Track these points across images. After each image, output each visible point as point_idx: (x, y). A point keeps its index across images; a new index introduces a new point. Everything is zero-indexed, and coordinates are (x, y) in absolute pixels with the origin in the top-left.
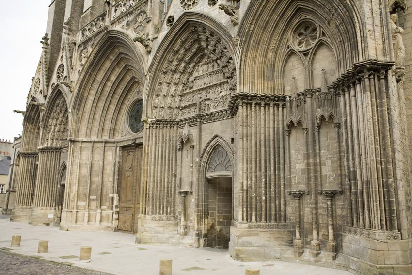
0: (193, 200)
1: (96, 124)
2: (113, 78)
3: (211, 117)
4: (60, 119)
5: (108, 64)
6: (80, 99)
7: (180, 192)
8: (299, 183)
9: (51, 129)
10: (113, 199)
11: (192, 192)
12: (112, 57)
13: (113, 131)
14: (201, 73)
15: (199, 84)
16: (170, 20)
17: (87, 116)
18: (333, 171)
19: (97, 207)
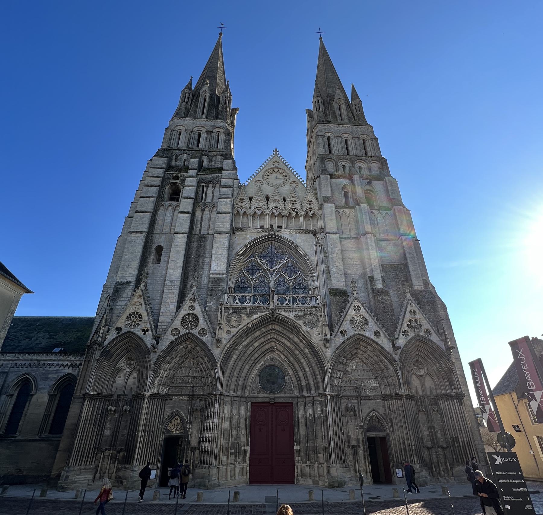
0: (361, 452)
1: (234, 380)
2: (256, 344)
3: (367, 398)
4: (172, 364)
5: (258, 333)
6: (227, 357)
7: (349, 446)
8: (427, 442)
9: (160, 373)
10: (246, 451)
11: (359, 446)
12: (264, 330)
13: (244, 387)
14: (354, 367)
15: (356, 374)
16: (344, 333)
17: (228, 372)
18: (442, 436)
19: (235, 460)
